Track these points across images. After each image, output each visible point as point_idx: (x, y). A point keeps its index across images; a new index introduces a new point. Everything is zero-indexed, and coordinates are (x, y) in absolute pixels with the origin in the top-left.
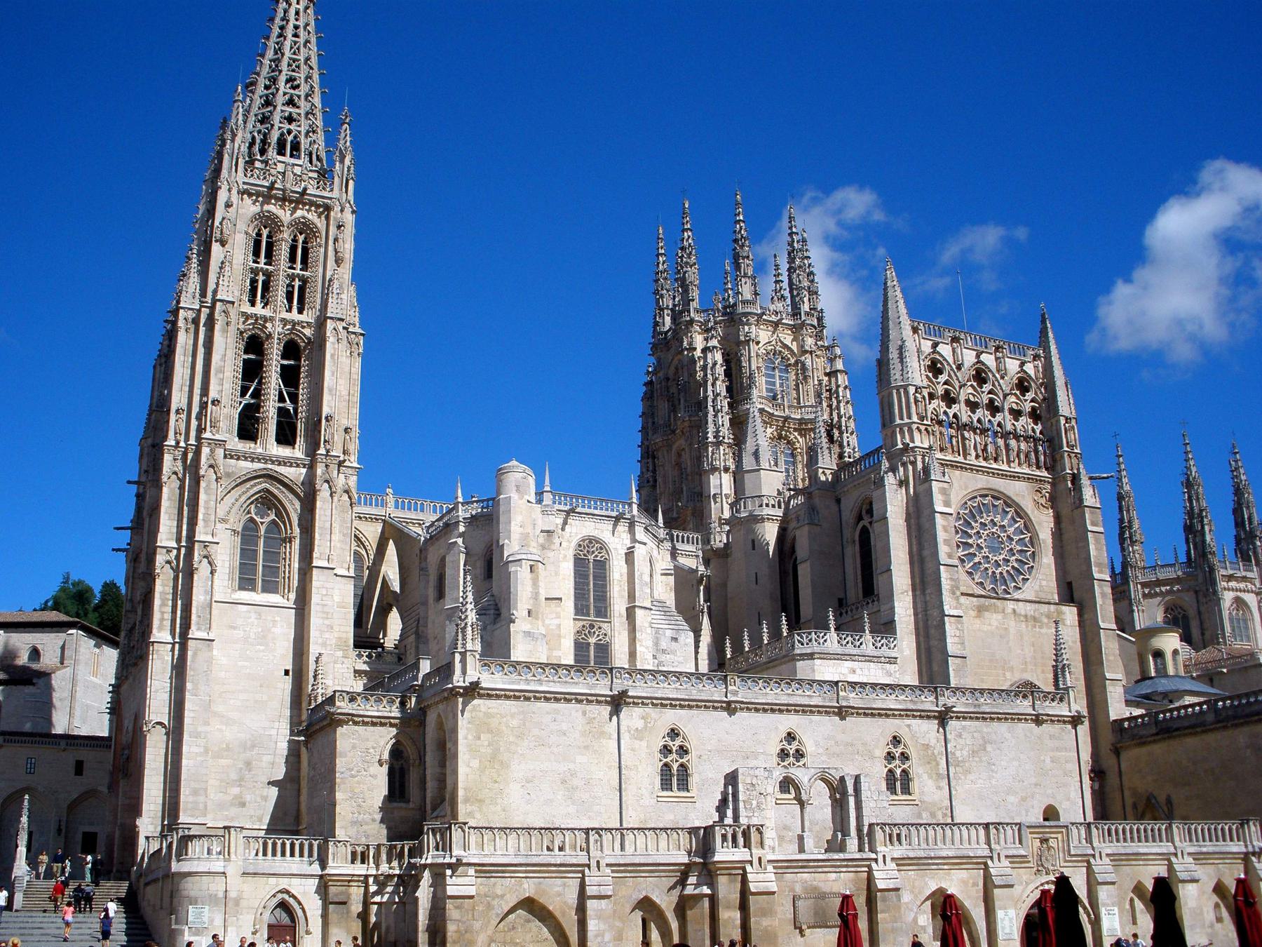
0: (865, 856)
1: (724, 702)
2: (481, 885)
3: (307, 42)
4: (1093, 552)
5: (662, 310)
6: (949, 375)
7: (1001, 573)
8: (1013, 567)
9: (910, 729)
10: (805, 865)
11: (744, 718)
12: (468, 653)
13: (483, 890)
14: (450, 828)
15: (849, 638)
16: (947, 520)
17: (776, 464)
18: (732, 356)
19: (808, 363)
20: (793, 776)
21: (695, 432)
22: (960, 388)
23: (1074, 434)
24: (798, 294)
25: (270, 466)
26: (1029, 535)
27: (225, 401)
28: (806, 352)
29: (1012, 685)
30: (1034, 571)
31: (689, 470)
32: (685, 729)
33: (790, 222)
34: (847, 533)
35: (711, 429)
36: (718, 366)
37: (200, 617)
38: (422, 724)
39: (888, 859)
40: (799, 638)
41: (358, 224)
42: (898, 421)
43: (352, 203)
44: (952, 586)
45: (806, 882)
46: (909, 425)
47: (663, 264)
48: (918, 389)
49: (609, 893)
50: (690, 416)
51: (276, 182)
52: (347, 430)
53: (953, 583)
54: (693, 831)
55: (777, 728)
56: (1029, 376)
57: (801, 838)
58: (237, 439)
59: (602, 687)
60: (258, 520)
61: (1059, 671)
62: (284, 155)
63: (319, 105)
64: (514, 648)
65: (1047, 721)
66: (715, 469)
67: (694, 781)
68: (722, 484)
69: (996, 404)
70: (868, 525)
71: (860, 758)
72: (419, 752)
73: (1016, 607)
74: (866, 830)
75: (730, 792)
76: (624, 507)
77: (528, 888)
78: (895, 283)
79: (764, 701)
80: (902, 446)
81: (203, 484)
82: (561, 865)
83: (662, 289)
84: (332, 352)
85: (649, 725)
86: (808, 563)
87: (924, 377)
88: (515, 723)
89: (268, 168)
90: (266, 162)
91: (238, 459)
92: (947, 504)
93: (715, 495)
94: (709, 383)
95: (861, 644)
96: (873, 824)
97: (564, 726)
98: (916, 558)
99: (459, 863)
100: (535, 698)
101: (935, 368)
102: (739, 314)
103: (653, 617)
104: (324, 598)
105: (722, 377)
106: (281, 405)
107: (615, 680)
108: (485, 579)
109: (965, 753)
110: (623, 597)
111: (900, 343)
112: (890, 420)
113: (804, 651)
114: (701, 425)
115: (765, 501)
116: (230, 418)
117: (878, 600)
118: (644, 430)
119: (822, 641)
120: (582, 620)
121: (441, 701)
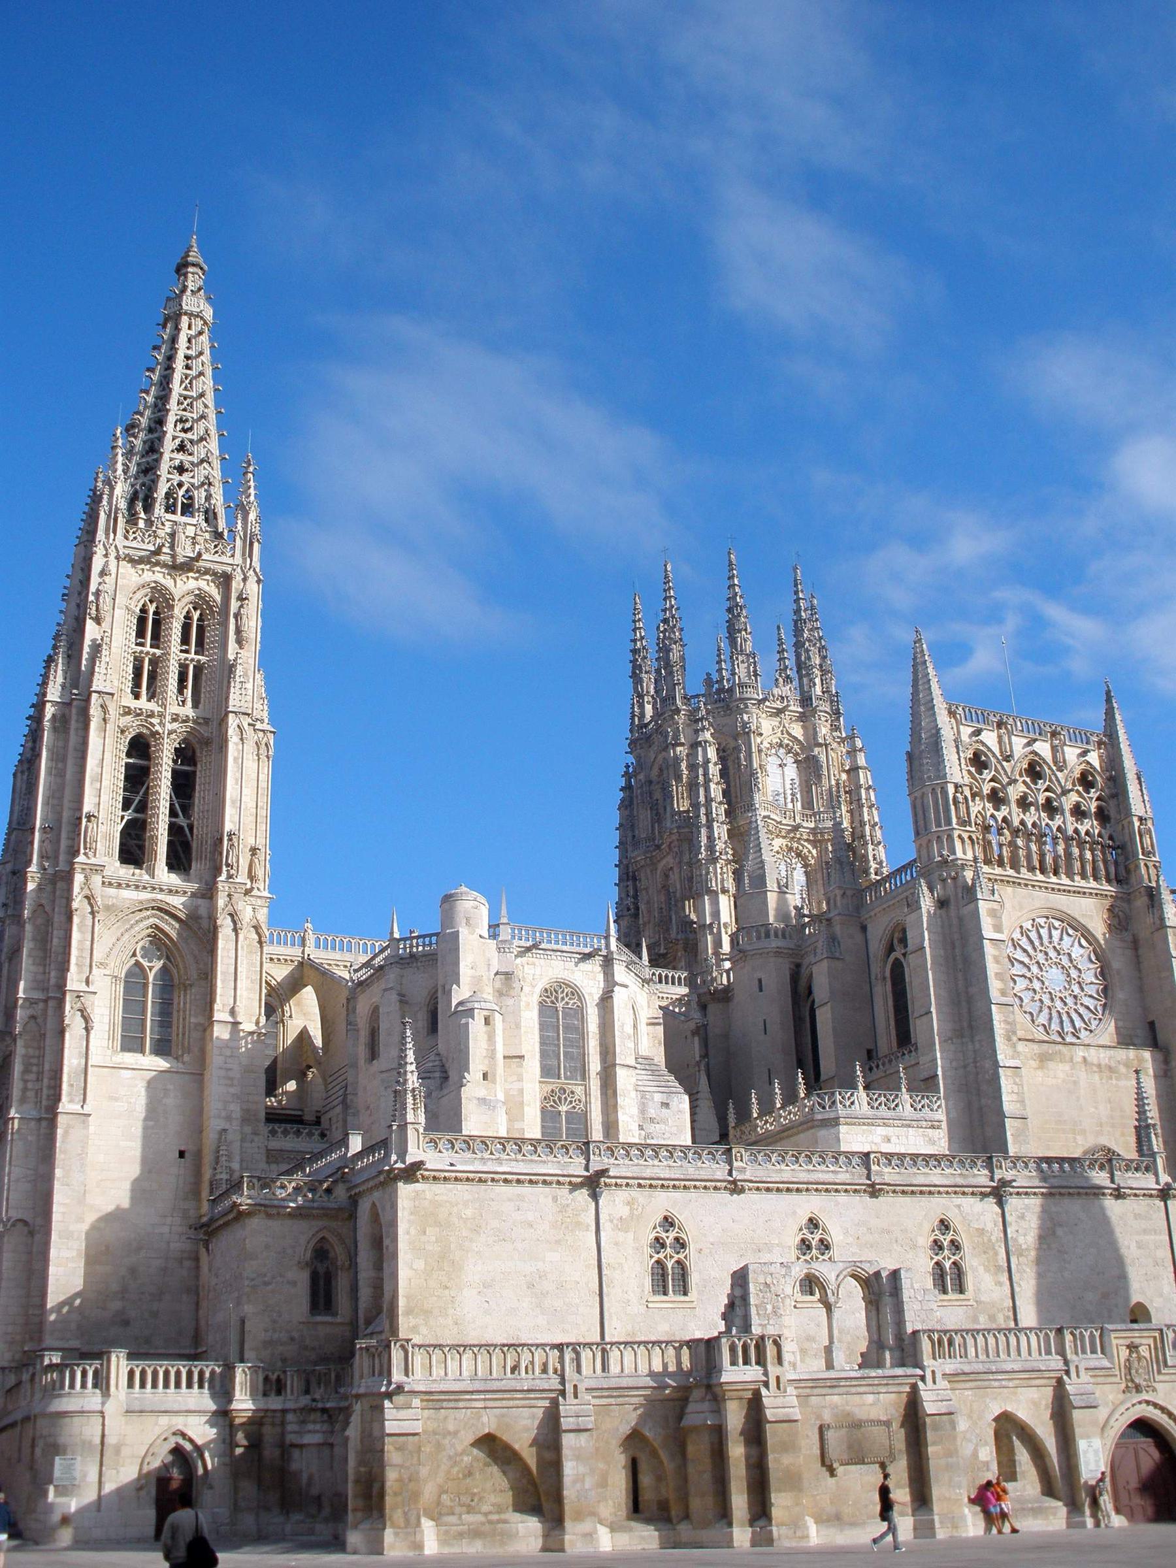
1: (729, 1182)
2: (428, 1418)
3: (201, 374)
5: (641, 696)
6: (996, 770)
8: (1082, 1004)
9: (960, 1211)
10: (834, 1384)
12: (410, 1127)
13: (431, 1425)
14: (389, 1346)
16: (999, 949)
18: (728, 752)
19: (823, 758)
20: (817, 1273)
23: (1151, 838)
25: (159, 897)
27: (102, 816)
29: (1085, 1153)
31: (678, 895)
32: (681, 1216)
33: (796, 585)
34: (875, 969)
36: (711, 765)
37: (72, 1085)
38: (352, 1216)
39: (938, 1376)
41: (266, 596)
42: (934, 829)
43: (258, 570)
44: (1007, 1031)
45: (837, 1407)
48: (957, 786)
51: (163, 545)
52: (254, 851)
54: (691, 1344)
55: (794, 1213)
56: (1095, 769)
57: (828, 1350)
58: (118, 864)
59: (576, 1167)
60: (146, 964)
61: (1142, 1132)
62: (174, 512)
63: (216, 452)
64: (466, 1119)
65: (1129, 1195)
67: (694, 1279)
70: (902, 959)
71: (899, 1249)
72: (349, 1253)
73: (1086, 1055)
76: (599, 942)
77: (488, 1423)
79: (778, 1180)
81: (76, 920)
82: (529, 1391)
84: (236, 754)
85: (635, 1212)
87: (965, 773)
88: (469, 1212)
89: (154, 528)
90: (149, 523)
91: (119, 886)
92: (998, 928)
93: (711, 924)
95: (897, 1105)
96: (918, 1331)
97: (530, 1216)
99: (400, 1389)
100: (493, 1180)
101: (979, 762)
102: (736, 701)
103: (640, 1077)
104: (229, 1060)
105: (717, 778)
106: (173, 820)
107: (592, 1157)
108: (428, 1034)
113: (826, 1116)
116: (108, 838)
117: (916, 1049)
118: (622, 846)
119: (848, 1103)
120: (550, 1083)
121: (376, 1187)
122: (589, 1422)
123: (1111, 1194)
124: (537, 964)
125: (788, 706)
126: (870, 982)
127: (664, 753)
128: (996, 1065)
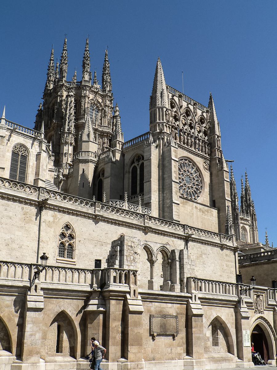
0: (183, 294)
4: (226, 189)
5: (50, 81)
6: (177, 109)
7: (190, 192)
8: (194, 190)
11: (101, 224)
15: (133, 206)
17: (96, 141)
19: (107, 109)
20: (149, 247)
21: (59, 128)
22: (181, 115)
24: (106, 84)
26: (201, 179)
28: (106, 106)
30: (201, 193)
33: (106, 56)
34: (126, 169)
35: (67, 127)
36: (72, 103)
40: (112, 203)
42: (158, 121)
46: (162, 124)
47: (52, 64)
49: (42, 307)
50: (58, 122)
53: (177, 190)
55: (116, 232)
56: (205, 118)
65: (225, 248)
66: (66, 143)
67: (76, 253)
68: (68, 149)
69: (192, 125)
74: (185, 280)
75: (119, 250)
78: (161, 67)
80: (159, 131)
83: (51, 73)
86: (110, 177)
92: (176, 157)
93: (65, 153)
94: (68, 109)
97: (11, 214)
98: (161, 178)
102: (83, 85)
105: (73, 108)
107: (41, 194)
109: (195, 258)
110: (33, 174)
111: (161, 90)
112: (154, 120)
114: (62, 125)
115: (90, 154)
122: (41, 305)
123: (220, 246)
124: (14, 136)
125: (99, 91)
126: (124, 173)
127: (55, 99)
128: (172, 202)
